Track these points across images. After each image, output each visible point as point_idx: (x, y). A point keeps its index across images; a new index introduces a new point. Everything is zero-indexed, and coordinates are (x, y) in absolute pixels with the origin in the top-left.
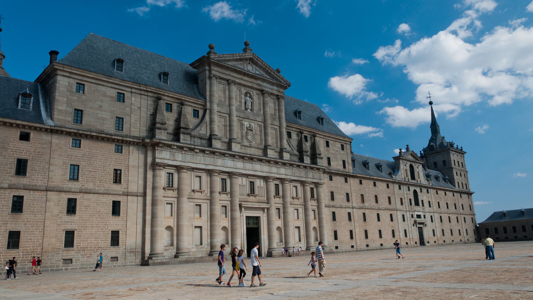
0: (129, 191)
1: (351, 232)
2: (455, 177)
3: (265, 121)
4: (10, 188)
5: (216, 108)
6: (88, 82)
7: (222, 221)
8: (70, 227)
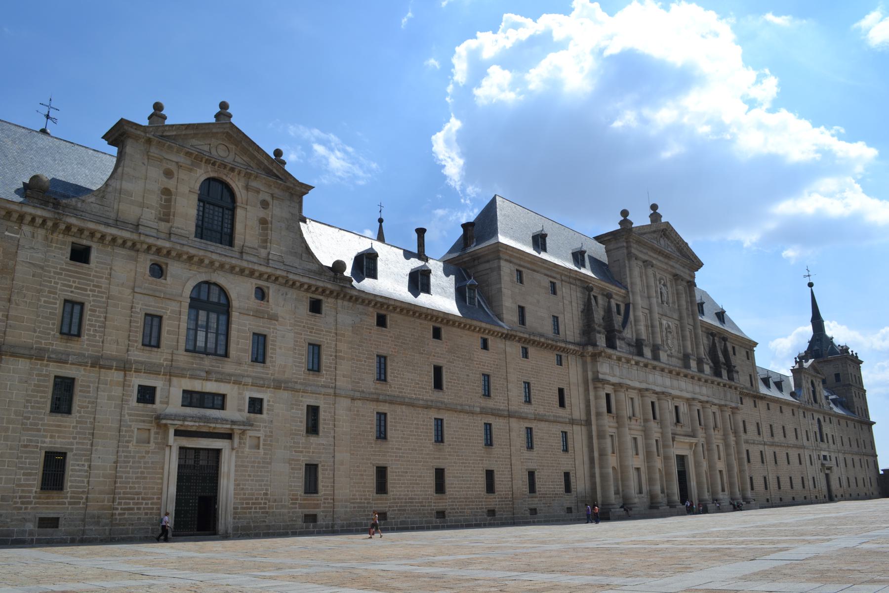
0: (574, 417)
1: (765, 478)
2: (855, 399)
3: (681, 318)
4: (484, 412)
5: (639, 300)
6: (528, 269)
7: (658, 463)
8: (532, 466)
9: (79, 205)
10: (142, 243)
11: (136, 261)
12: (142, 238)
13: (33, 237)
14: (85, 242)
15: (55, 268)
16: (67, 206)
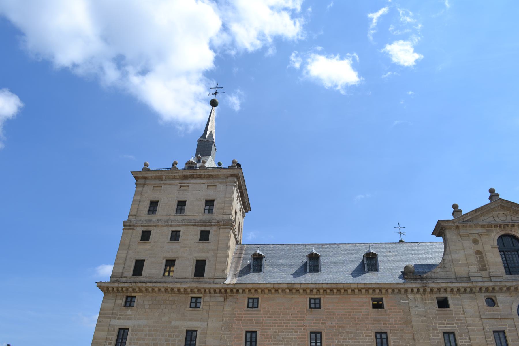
9: (433, 275)
10: (476, 287)
11: (476, 299)
12: (475, 284)
13: (415, 300)
14: (443, 296)
15: (432, 315)
16: (427, 278)
